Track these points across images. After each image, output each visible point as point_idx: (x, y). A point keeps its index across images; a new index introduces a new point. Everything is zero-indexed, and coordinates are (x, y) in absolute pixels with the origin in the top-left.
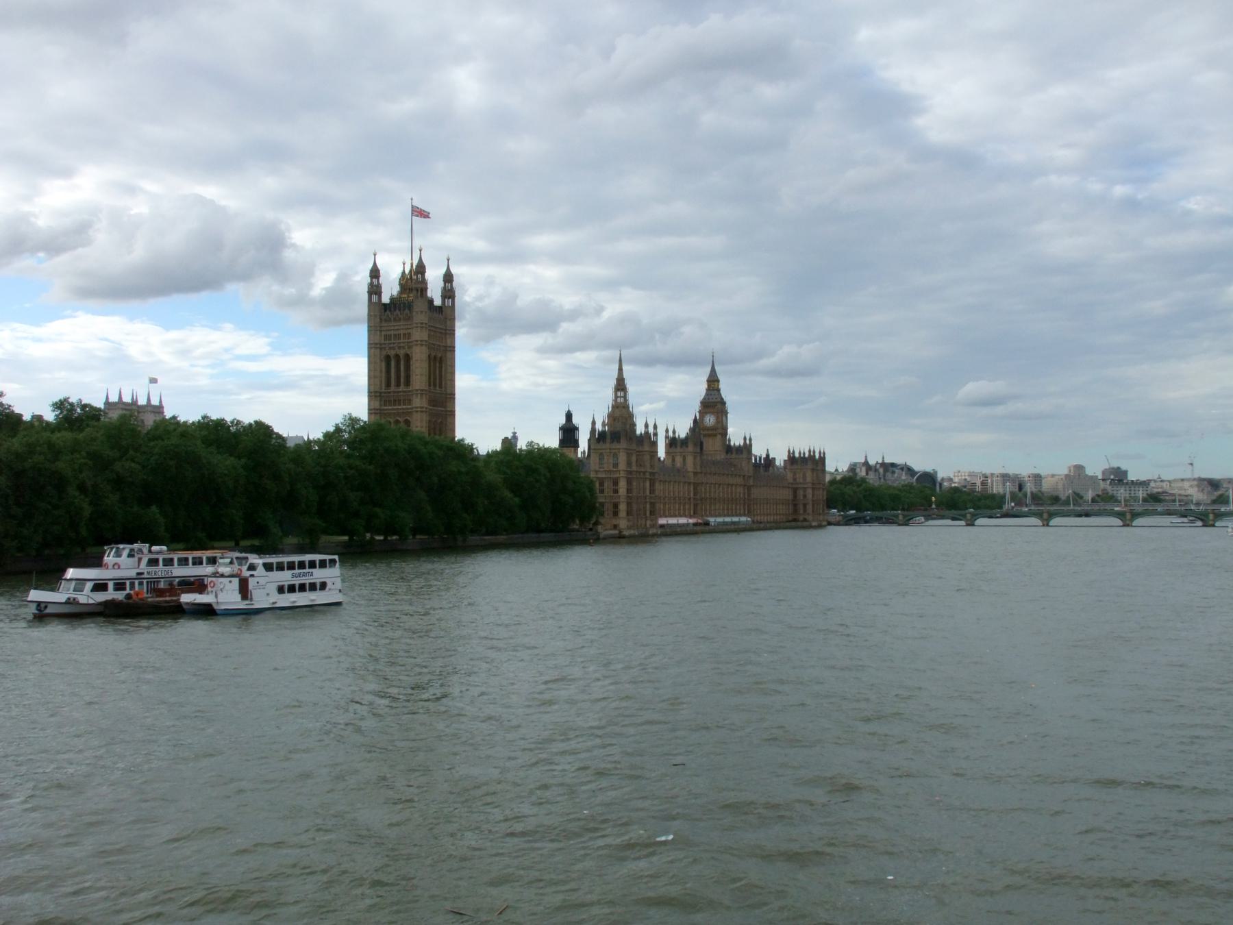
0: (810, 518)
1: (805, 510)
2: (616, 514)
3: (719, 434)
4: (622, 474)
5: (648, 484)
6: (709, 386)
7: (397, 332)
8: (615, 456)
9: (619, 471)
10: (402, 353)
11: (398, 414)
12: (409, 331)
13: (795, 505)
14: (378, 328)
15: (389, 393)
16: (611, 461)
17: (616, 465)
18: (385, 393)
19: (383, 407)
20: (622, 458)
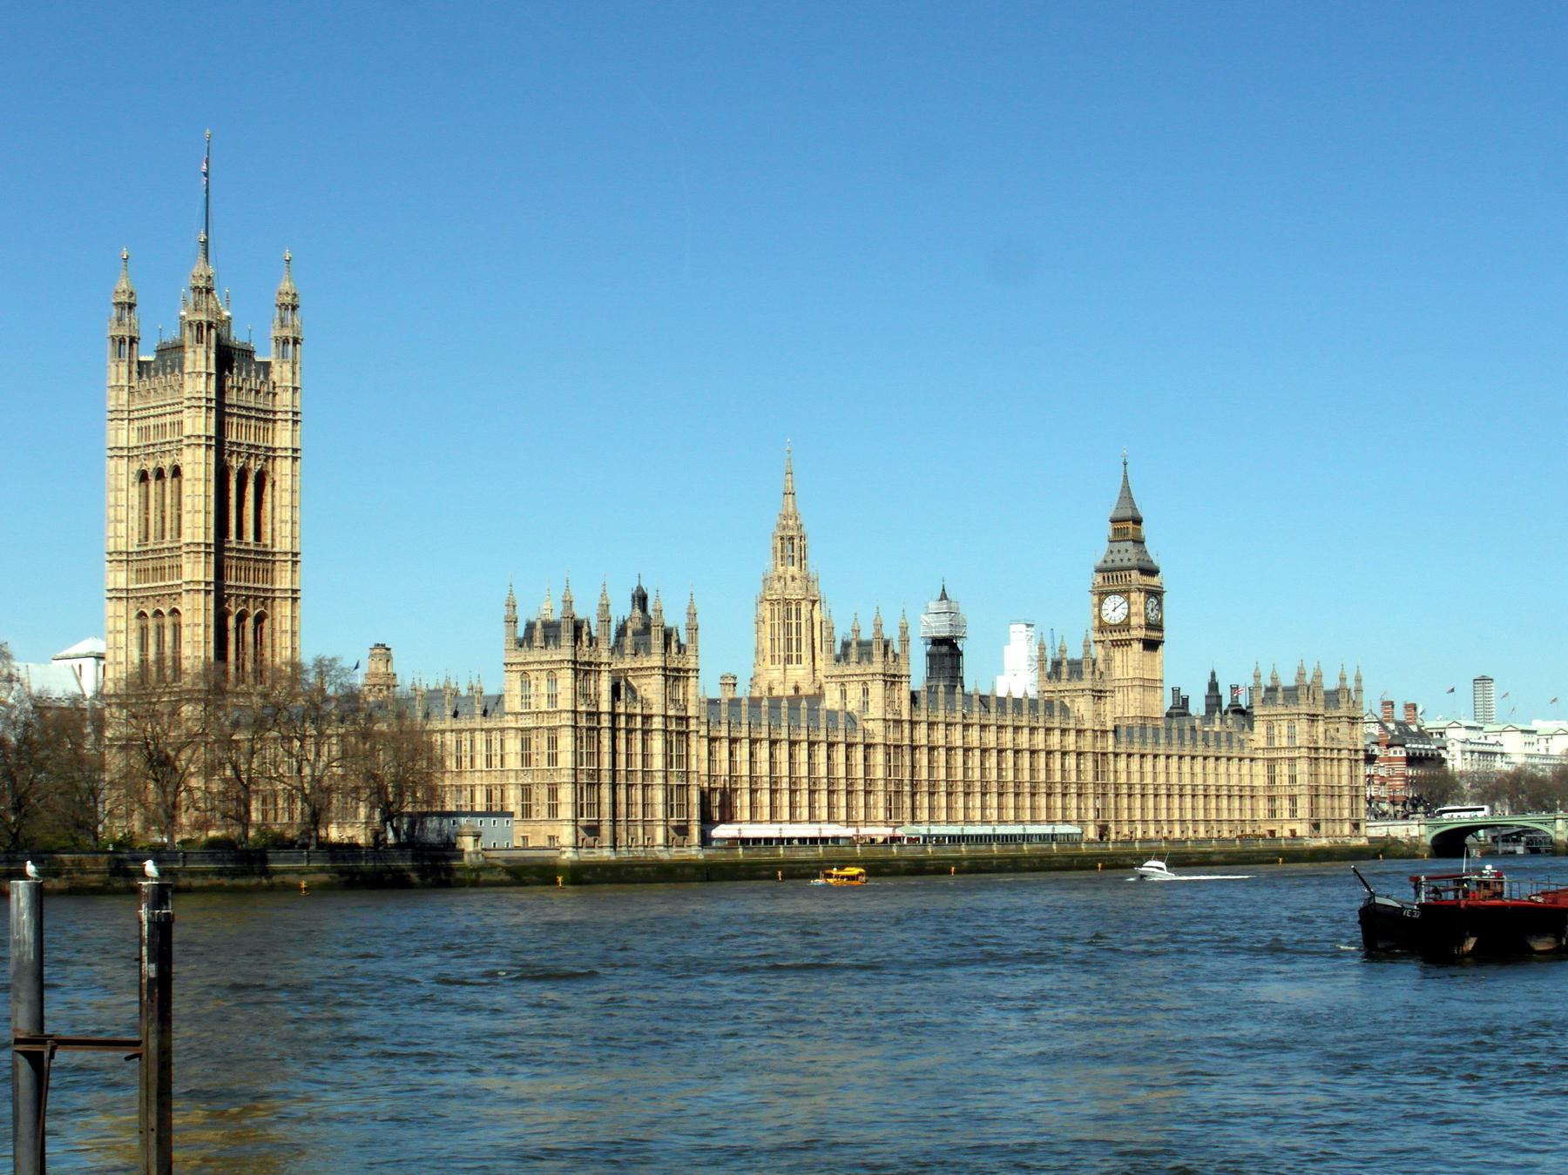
0: (1302, 829)
1: (1293, 812)
2: (553, 810)
3: (1139, 640)
4: (567, 719)
5: (657, 744)
6: (1116, 531)
7: (161, 421)
8: (553, 681)
9: (560, 711)
10: (166, 463)
11: (159, 598)
12: (177, 418)
13: (1272, 799)
14: (125, 415)
15: (145, 552)
16: (544, 688)
17: (553, 698)
18: (138, 553)
19: (131, 587)
20: (566, 679)
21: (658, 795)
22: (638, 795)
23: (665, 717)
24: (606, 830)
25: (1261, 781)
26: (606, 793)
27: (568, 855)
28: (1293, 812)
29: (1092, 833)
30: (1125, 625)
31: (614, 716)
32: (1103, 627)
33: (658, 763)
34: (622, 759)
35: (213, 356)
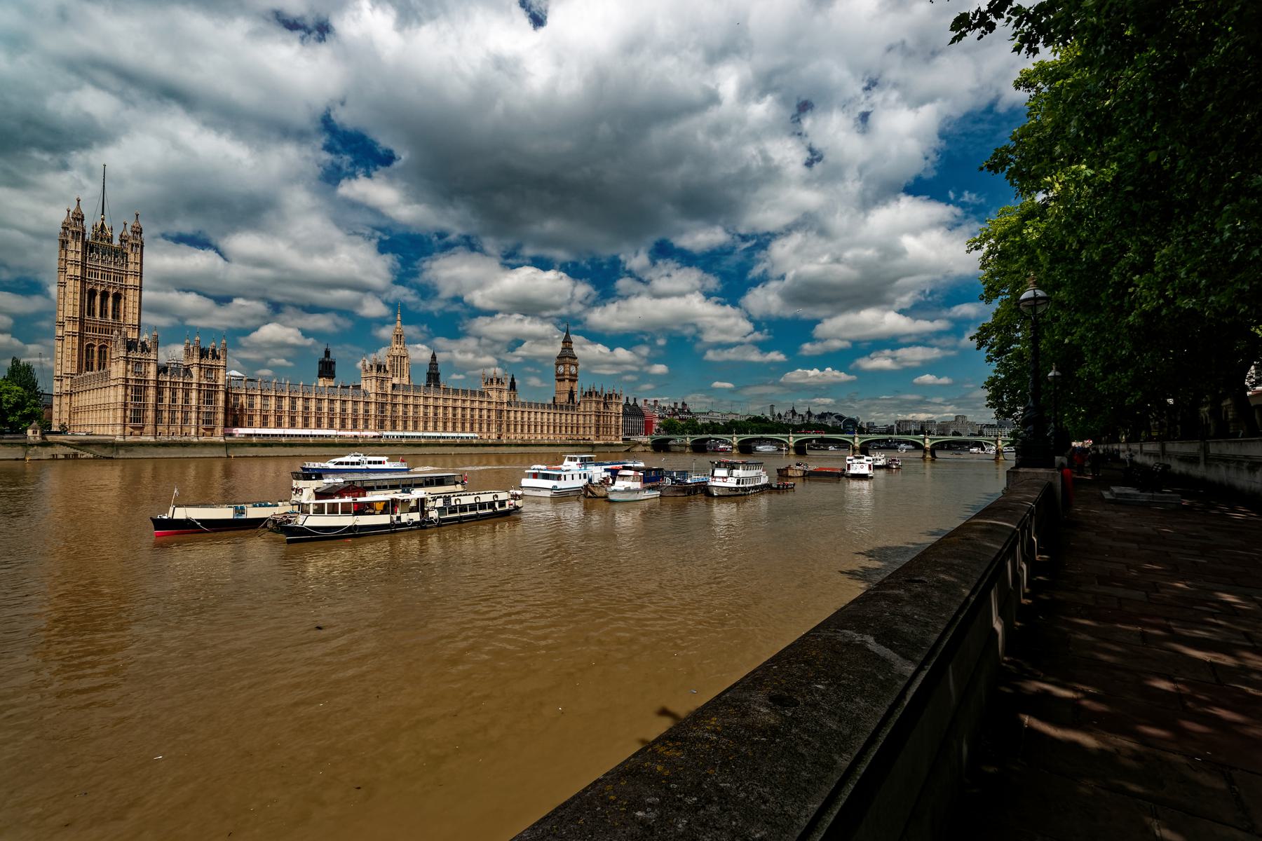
0: (592, 438)
1: (590, 432)
5: (194, 395)
21: (194, 415)
22: (179, 415)
23: (200, 385)
24: (149, 428)
25: (581, 422)
26: (150, 414)
27: (119, 439)
28: (590, 432)
29: (494, 436)
30: (563, 374)
31: (158, 382)
32: (558, 375)
33: (194, 402)
34: (167, 401)
35: (80, 244)
